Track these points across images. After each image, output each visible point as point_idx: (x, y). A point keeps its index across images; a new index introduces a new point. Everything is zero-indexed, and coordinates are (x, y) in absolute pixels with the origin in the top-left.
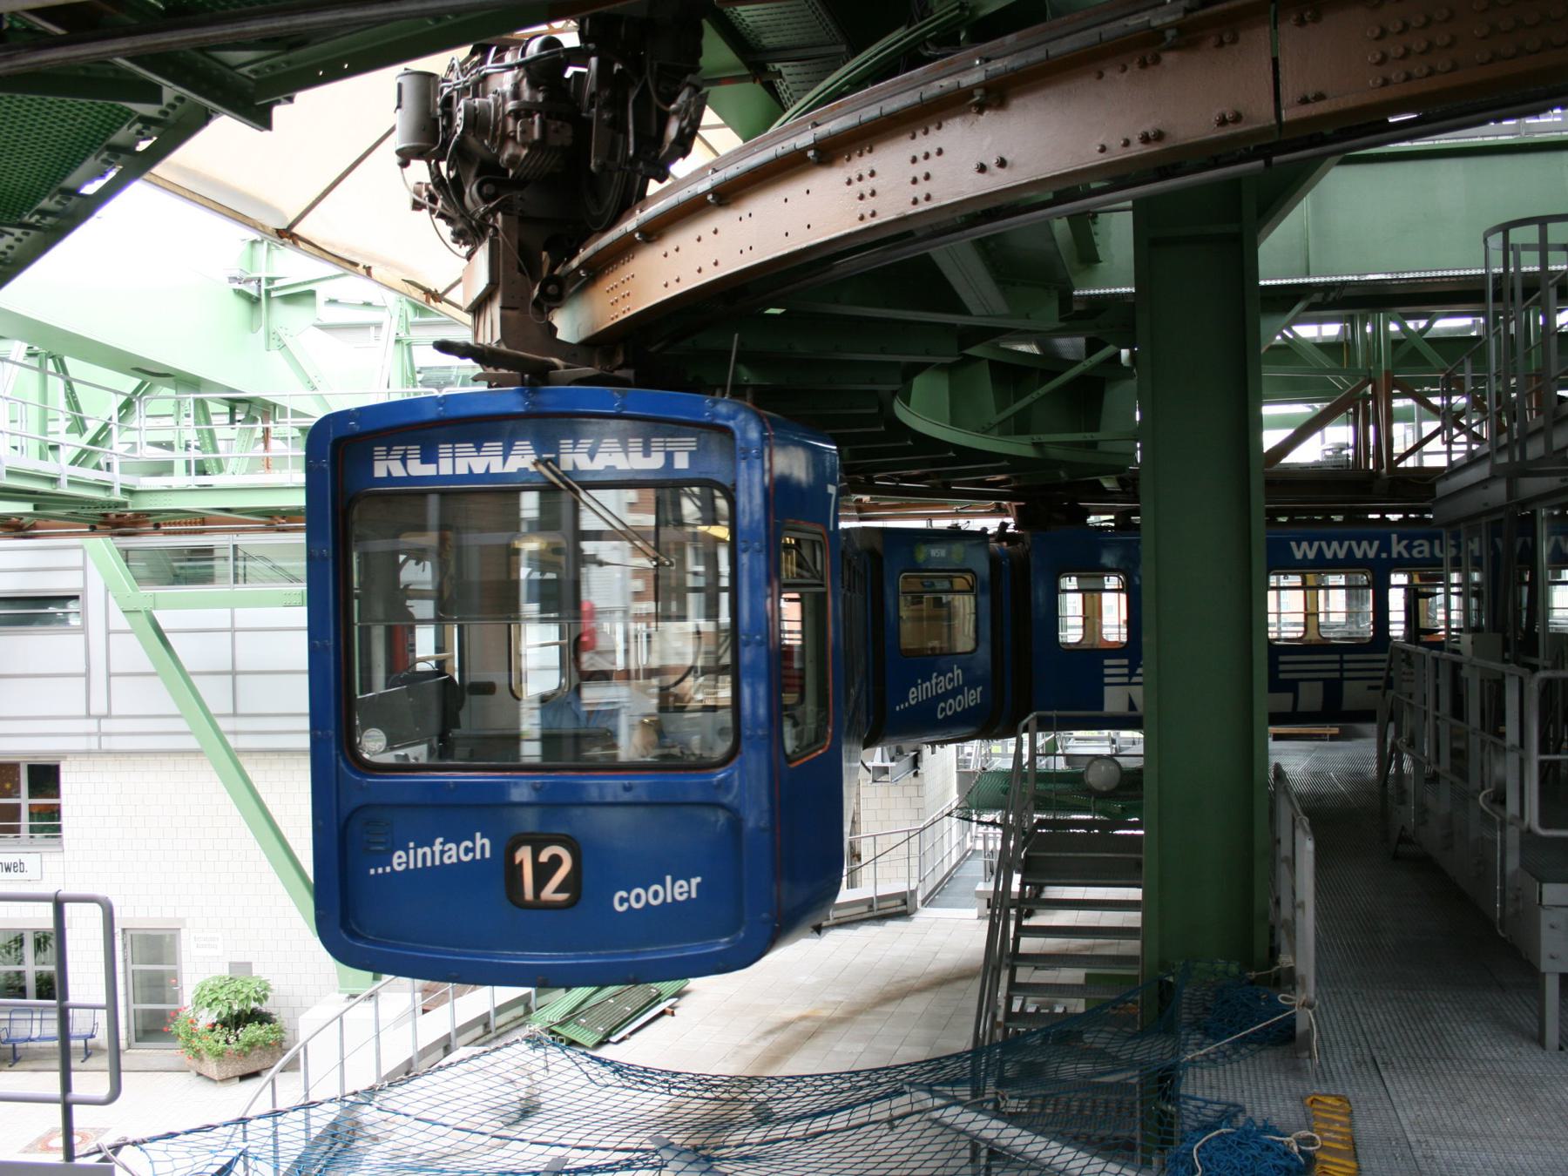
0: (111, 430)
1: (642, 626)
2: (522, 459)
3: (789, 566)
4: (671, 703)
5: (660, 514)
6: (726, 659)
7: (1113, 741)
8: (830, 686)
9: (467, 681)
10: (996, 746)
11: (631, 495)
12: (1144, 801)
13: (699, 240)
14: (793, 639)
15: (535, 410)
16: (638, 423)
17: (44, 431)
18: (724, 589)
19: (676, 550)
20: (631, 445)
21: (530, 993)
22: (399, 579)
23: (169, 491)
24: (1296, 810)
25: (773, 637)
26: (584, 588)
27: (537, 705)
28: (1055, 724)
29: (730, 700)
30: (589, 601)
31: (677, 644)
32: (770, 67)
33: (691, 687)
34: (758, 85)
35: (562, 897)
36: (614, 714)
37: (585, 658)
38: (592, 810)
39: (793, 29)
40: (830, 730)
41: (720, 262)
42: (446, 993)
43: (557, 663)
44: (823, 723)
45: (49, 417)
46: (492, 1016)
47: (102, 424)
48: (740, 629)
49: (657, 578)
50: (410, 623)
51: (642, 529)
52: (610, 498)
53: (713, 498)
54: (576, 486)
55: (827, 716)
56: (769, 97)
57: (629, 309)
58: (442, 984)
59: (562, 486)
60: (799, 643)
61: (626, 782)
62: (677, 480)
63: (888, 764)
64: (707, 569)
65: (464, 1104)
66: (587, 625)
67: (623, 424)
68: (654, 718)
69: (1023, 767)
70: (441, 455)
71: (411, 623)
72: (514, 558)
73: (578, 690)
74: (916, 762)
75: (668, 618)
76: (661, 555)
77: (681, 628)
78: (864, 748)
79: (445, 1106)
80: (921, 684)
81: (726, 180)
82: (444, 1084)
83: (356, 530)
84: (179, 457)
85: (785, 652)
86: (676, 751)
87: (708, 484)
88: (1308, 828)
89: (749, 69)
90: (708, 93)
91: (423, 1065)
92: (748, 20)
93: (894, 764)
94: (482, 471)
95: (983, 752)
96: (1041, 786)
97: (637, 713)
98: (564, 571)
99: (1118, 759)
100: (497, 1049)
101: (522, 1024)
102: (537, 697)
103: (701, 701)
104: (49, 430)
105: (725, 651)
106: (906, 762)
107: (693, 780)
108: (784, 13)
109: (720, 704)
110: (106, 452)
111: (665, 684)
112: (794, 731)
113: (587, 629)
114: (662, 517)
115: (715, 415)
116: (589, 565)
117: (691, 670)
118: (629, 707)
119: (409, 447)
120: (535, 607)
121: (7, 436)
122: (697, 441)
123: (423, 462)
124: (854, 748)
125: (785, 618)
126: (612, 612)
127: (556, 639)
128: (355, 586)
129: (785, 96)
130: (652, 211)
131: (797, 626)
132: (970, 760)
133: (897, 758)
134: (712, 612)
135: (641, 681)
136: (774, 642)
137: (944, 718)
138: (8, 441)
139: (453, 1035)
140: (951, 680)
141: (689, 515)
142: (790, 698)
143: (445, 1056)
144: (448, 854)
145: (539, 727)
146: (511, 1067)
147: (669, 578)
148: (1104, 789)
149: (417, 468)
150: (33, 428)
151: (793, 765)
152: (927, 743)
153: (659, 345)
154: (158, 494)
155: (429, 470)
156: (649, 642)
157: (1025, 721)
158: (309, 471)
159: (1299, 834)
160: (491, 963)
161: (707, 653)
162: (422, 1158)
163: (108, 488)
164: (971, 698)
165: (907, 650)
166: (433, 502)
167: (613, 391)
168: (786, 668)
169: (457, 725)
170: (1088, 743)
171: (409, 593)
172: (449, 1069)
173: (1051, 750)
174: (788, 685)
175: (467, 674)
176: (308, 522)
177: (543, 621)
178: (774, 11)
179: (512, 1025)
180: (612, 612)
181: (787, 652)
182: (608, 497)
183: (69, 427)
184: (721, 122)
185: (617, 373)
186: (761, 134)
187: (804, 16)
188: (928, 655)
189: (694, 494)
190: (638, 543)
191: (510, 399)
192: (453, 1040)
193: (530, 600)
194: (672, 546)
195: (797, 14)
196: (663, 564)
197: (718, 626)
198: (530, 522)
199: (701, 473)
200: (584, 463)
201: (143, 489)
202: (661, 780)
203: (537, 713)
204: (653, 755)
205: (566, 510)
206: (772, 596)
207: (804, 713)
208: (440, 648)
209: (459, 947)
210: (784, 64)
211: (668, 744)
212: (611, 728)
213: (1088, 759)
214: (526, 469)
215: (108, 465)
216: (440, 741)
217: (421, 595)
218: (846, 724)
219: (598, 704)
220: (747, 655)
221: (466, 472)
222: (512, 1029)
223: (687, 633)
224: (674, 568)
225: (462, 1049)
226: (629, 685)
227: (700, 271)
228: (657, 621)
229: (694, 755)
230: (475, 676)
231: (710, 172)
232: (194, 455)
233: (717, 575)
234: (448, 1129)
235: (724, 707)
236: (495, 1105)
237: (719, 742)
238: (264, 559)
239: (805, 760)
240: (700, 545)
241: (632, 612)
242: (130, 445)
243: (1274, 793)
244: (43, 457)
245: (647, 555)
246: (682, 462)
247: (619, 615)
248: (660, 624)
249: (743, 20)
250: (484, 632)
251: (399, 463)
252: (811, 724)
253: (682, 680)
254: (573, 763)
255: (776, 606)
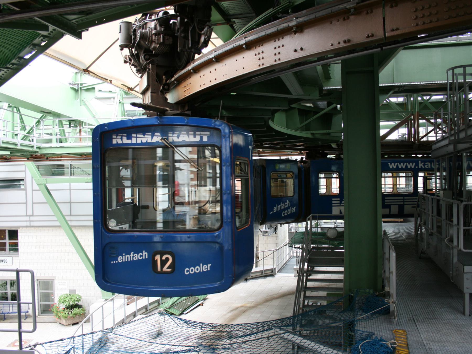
0: (33, 129)
1: (193, 189)
2: (157, 138)
3: (238, 170)
4: (202, 212)
5: (199, 155)
6: (219, 199)
7: (335, 223)
8: (250, 206)
9: (141, 205)
10: (300, 225)
11: (190, 149)
12: (344, 241)
13: (210, 72)
14: (239, 192)
15: (161, 123)
16: (192, 127)
17: (13, 130)
18: (218, 177)
19: (203, 165)
20: (190, 134)
21: (159, 299)
22: (120, 174)
23: (51, 148)
24: (390, 244)
25: (233, 192)
26: (176, 177)
27: (162, 212)
28: (318, 218)
29: (220, 211)
30: (177, 181)
31: (204, 194)
32: (232, 20)
33: (208, 207)
34: (228, 26)
35: (169, 270)
36: (185, 215)
37: (176, 198)
38: (178, 244)
39: (239, 9)
40: (250, 220)
41: (217, 79)
42: (134, 299)
43: (168, 200)
44: (248, 218)
45: (15, 126)
46: (148, 306)
47: (31, 128)
48: (223, 189)
49: (198, 174)
50: (124, 188)
51: (193, 159)
52: (184, 150)
53: (215, 150)
54: (173, 146)
55: (249, 216)
56: (232, 29)
57: (189, 93)
58: (133, 296)
59: (169, 146)
60: (241, 193)
61: (189, 235)
62: (204, 145)
63: (267, 230)
64: (213, 171)
65: (140, 332)
66: (177, 188)
67: (188, 127)
68: (197, 216)
69: (308, 231)
70: (133, 137)
71: (124, 188)
72: (155, 168)
73: (174, 208)
74: (276, 229)
75: (201, 186)
76: (199, 167)
77: (205, 189)
78: (260, 225)
79: (134, 333)
80: (277, 206)
81: (219, 54)
82: (134, 326)
83: (107, 159)
84: (54, 138)
85: (236, 196)
86: (203, 226)
87: (213, 146)
88: (394, 249)
89: (226, 21)
90: (213, 28)
91: (127, 321)
92: (225, 6)
93: (269, 230)
94: (145, 142)
95: (296, 226)
96: (313, 237)
97: (192, 215)
98: (170, 172)
99: (337, 228)
100: (150, 316)
101: (157, 308)
102: (162, 210)
103: (211, 211)
104: (15, 129)
105: (218, 196)
106: (273, 230)
107: (209, 235)
108: (236, 4)
109: (217, 212)
110: (32, 136)
111: (200, 206)
112: (239, 220)
113: (177, 189)
114: (199, 156)
115: (215, 125)
116: (177, 170)
117: (208, 202)
118: (189, 213)
119: (123, 135)
120: (161, 183)
121: (2, 131)
122: (210, 133)
123: (127, 139)
124: (257, 225)
125: (236, 186)
126: (184, 184)
127: (167, 192)
128: (107, 176)
129: (236, 29)
130: (196, 63)
131: (240, 189)
132: (292, 229)
133: (270, 228)
134: (214, 184)
135: (193, 205)
136: (233, 193)
137: (284, 216)
138: (2, 133)
139: (136, 312)
140: (286, 205)
141: (207, 155)
142: (238, 210)
143: (134, 318)
144: (135, 257)
145: (162, 219)
146: (154, 321)
147: (201, 174)
148: (332, 237)
149: (126, 141)
150: (10, 129)
151: (239, 230)
152: (279, 224)
153: (198, 104)
154: (48, 149)
155: (129, 141)
156: (195, 193)
157: (309, 217)
158: (93, 142)
159: (391, 251)
160: (148, 290)
161: (213, 197)
162: (127, 348)
163: (32, 147)
164: (292, 210)
165: (273, 196)
166: (130, 151)
167: (185, 118)
168: (237, 201)
169: (138, 218)
170: (327, 224)
171: (123, 178)
172: (135, 322)
173: (316, 226)
174: (237, 206)
175: (140, 203)
176: (93, 157)
177: (163, 187)
178: (233, 3)
179: (154, 309)
180: (184, 184)
181: (237, 196)
182: (183, 150)
183: (21, 129)
184: (217, 37)
185: (186, 112)
186: (229, 40)
187: (242, 5)
188: (279, 197)
189: (209, 149)
190: (192, 163)
191: (154, 120)
192: (136, 313)
193: (159, 181)
194: (202, 164)
195: (240, 4)
196: (200, 170)
197: (216, 188)
198: (160, 157)
199: (211, 142)
200: (176, 139)
201: (43, 147)
202: (199, 235)
203: (162, 215)
204: (196, 227)
205: (170, 154)
206: (232, 179)
207: (242, 215)
208: (132, 195)
209: (138, 285)
210: (236, 19)
211: (201, 224)
212: (184, 219)
213: (328, 228)
214: (158, 141)
215: (33, 140)
216: (132, 223)
217: (127, 179)
218: (255, 218)
219: (180, 212)
220: (225, 197)
221: (140, 142)
222: (154, 310)
223: (207, 191)
224: (203, 171)
225: (139, 316)
226: (189, 206)
227: (211, 81)
228: (198, 187)
229: (209, 227)
230: (143, 203)
231: (214, 52)
232: (58, 137)
233: (216, 173)
234: (135, 340)
235: (218, 213)
236: (149, 333)
237: (216, 223)
238: (80, 168)
239: (242, 229)
240: (211, 164)
241: (190, 184)
242: (39, 134)
243: (384, 239)
244: (13, 137)
245: (195, 167)
246: (205, 139)
247: (186, 185)
248: (199, 188)
249: (224, 6)
250: (146, 190)
251: (120, 139)
252: (244, 218)
253: (205, 205)
254: (172, 230)
255: (234, 182)
